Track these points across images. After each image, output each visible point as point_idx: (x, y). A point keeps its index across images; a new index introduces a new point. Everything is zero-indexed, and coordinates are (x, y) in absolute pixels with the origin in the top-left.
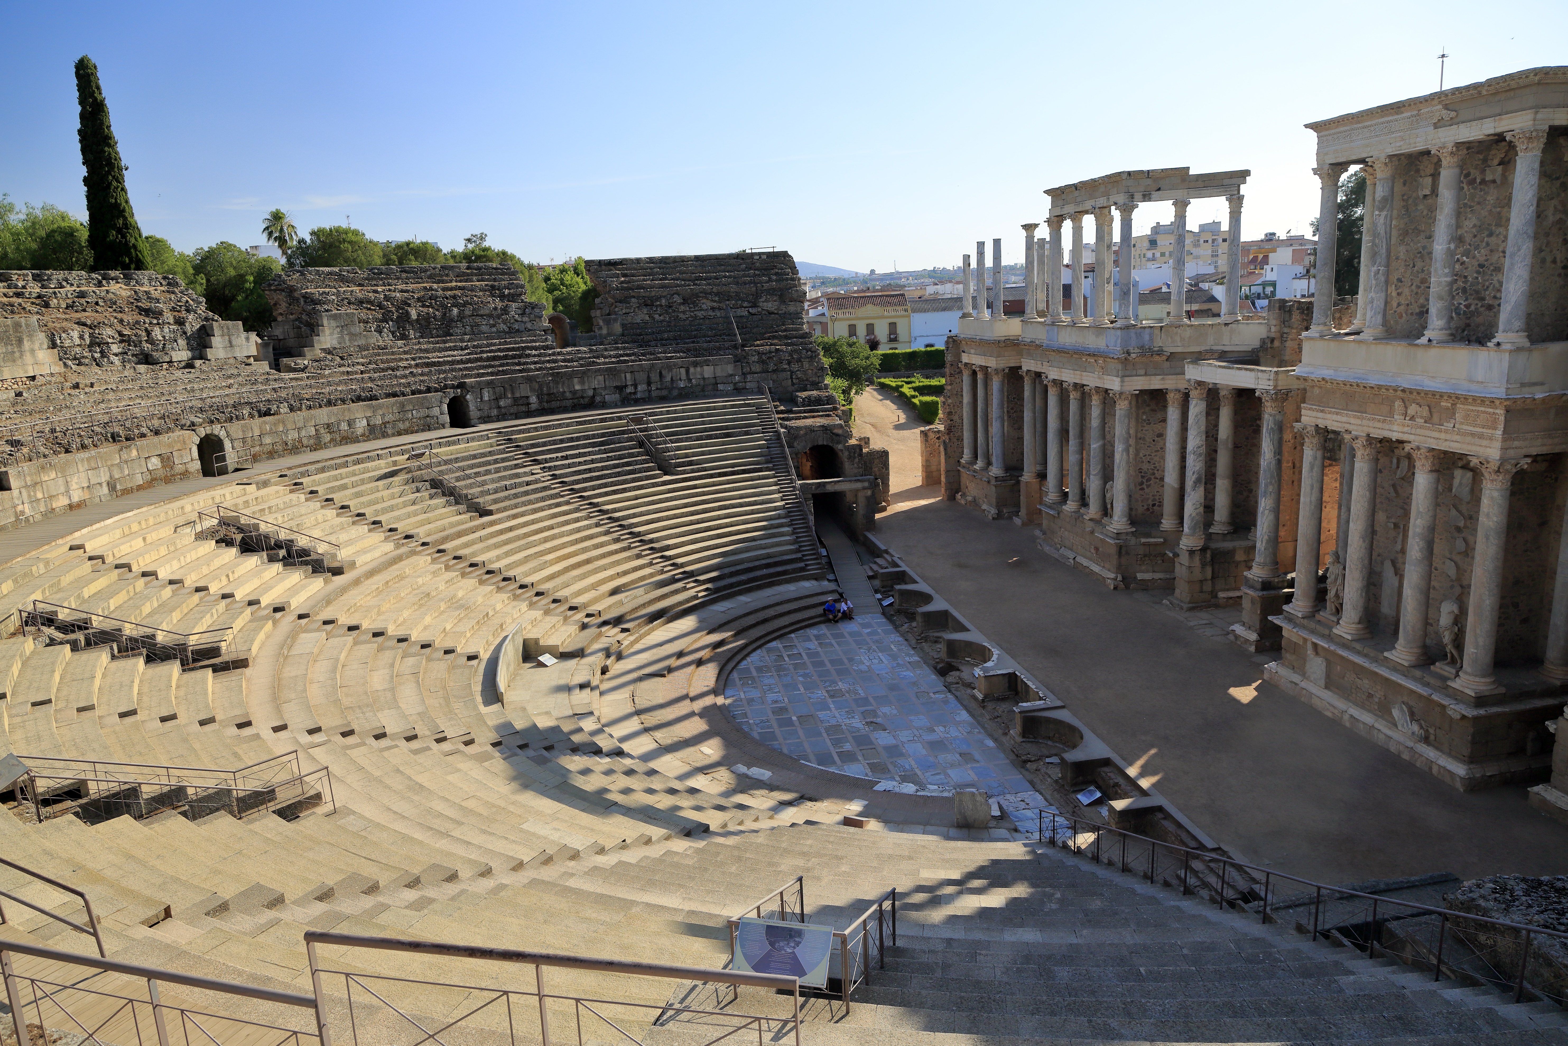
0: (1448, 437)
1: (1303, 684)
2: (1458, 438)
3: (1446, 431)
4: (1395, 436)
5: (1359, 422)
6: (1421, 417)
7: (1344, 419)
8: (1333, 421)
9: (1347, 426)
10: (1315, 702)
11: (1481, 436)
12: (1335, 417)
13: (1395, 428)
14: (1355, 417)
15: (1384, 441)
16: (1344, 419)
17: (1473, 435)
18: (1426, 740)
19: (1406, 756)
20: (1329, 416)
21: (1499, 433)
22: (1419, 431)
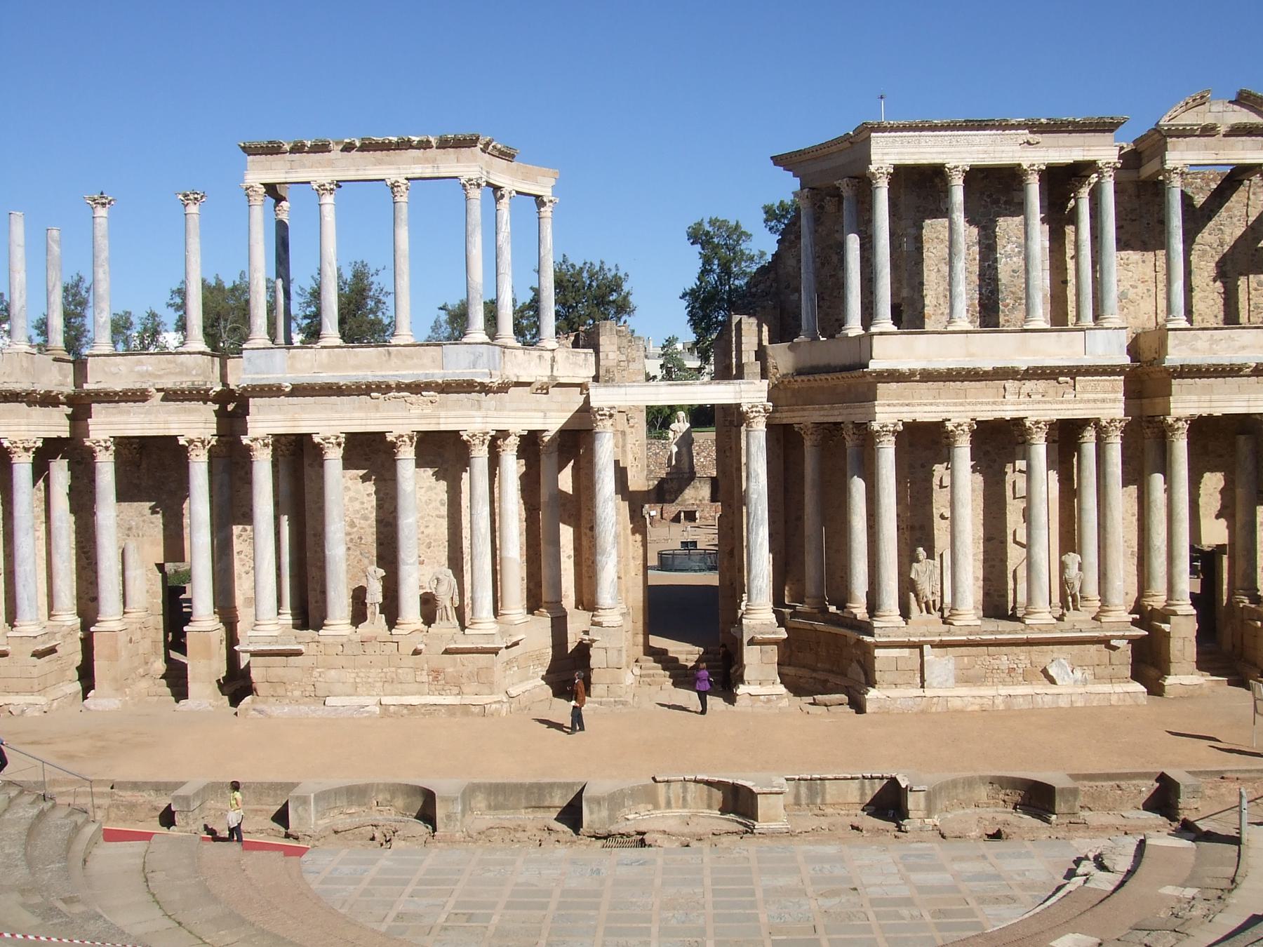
0: (1071, 406)
2: (1081, 406)
3: (1069, 402)
4: (1008, 416)
5: (962, 408)
6: (1038, 393)
8: (926, 412)
9: (945, 416)
11: (1104, 401)
13: (1008, 407)
14: (955, 404)
17: (1095, 401)
19: (1080, 703)
20: (918, 408)
21: (1121, 396)
22: (1036, 406)
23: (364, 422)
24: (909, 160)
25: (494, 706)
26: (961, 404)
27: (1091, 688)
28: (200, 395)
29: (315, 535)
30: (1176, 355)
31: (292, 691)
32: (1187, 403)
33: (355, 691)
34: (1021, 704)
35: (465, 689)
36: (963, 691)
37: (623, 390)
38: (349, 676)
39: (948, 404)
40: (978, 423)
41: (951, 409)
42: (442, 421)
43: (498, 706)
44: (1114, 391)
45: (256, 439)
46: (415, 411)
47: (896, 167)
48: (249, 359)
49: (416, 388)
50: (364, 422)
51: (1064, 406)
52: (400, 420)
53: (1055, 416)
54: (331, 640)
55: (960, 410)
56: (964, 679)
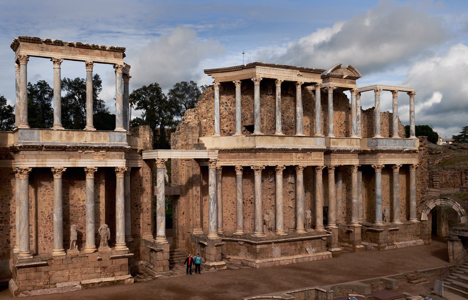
1: (274, 260)
4: (294, 165)
5: (281, 162)
7: (276, 162)
8: (271, 163)
9: (277, 164)
10: (282, 263)
11: (319, 160)
12: (272, 162)
13: (294, 162)
14: (279, 160)
15: (291, 166)
16: (276, 162)
17: (317, 160)
18: (316, 252)
20: (269, 162)
23: (74, 163)
24: (267, 77)
25: (129, 279)
26: (281, 160)
27: (318, 254)
28: (120, 149)
29: (42, 212)
30: (333, 147)
31: (39, 283)
32: (335, 162)
33: (69, 279)
34: (300, 261)
35: (116, 274)
36: (284, 258)
37: (170, 153)
38: (67, 273)
39: (277, 160)
40: (286, 167)
41: (279, 162)
42: (108, 163)
43: (131, 279)
44: (321, 157)
45: (25, 170)
46: (96, 158)
47: (264, 79)
48: (21, 134)
49: (97, 149)
50: (74, 163)
51: (309, 162)
52: (90, 163)
53: (305, 165)
54: (58, 258)
55: (281, 162)
56: (283, 254)
